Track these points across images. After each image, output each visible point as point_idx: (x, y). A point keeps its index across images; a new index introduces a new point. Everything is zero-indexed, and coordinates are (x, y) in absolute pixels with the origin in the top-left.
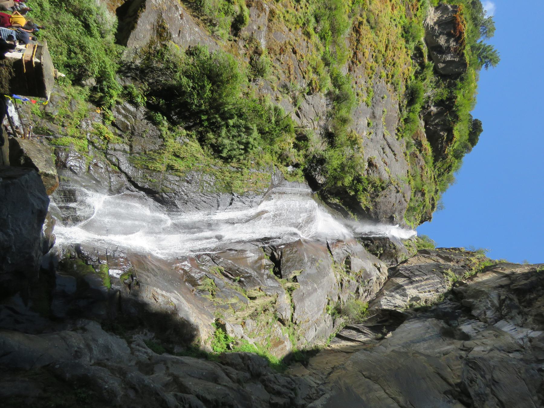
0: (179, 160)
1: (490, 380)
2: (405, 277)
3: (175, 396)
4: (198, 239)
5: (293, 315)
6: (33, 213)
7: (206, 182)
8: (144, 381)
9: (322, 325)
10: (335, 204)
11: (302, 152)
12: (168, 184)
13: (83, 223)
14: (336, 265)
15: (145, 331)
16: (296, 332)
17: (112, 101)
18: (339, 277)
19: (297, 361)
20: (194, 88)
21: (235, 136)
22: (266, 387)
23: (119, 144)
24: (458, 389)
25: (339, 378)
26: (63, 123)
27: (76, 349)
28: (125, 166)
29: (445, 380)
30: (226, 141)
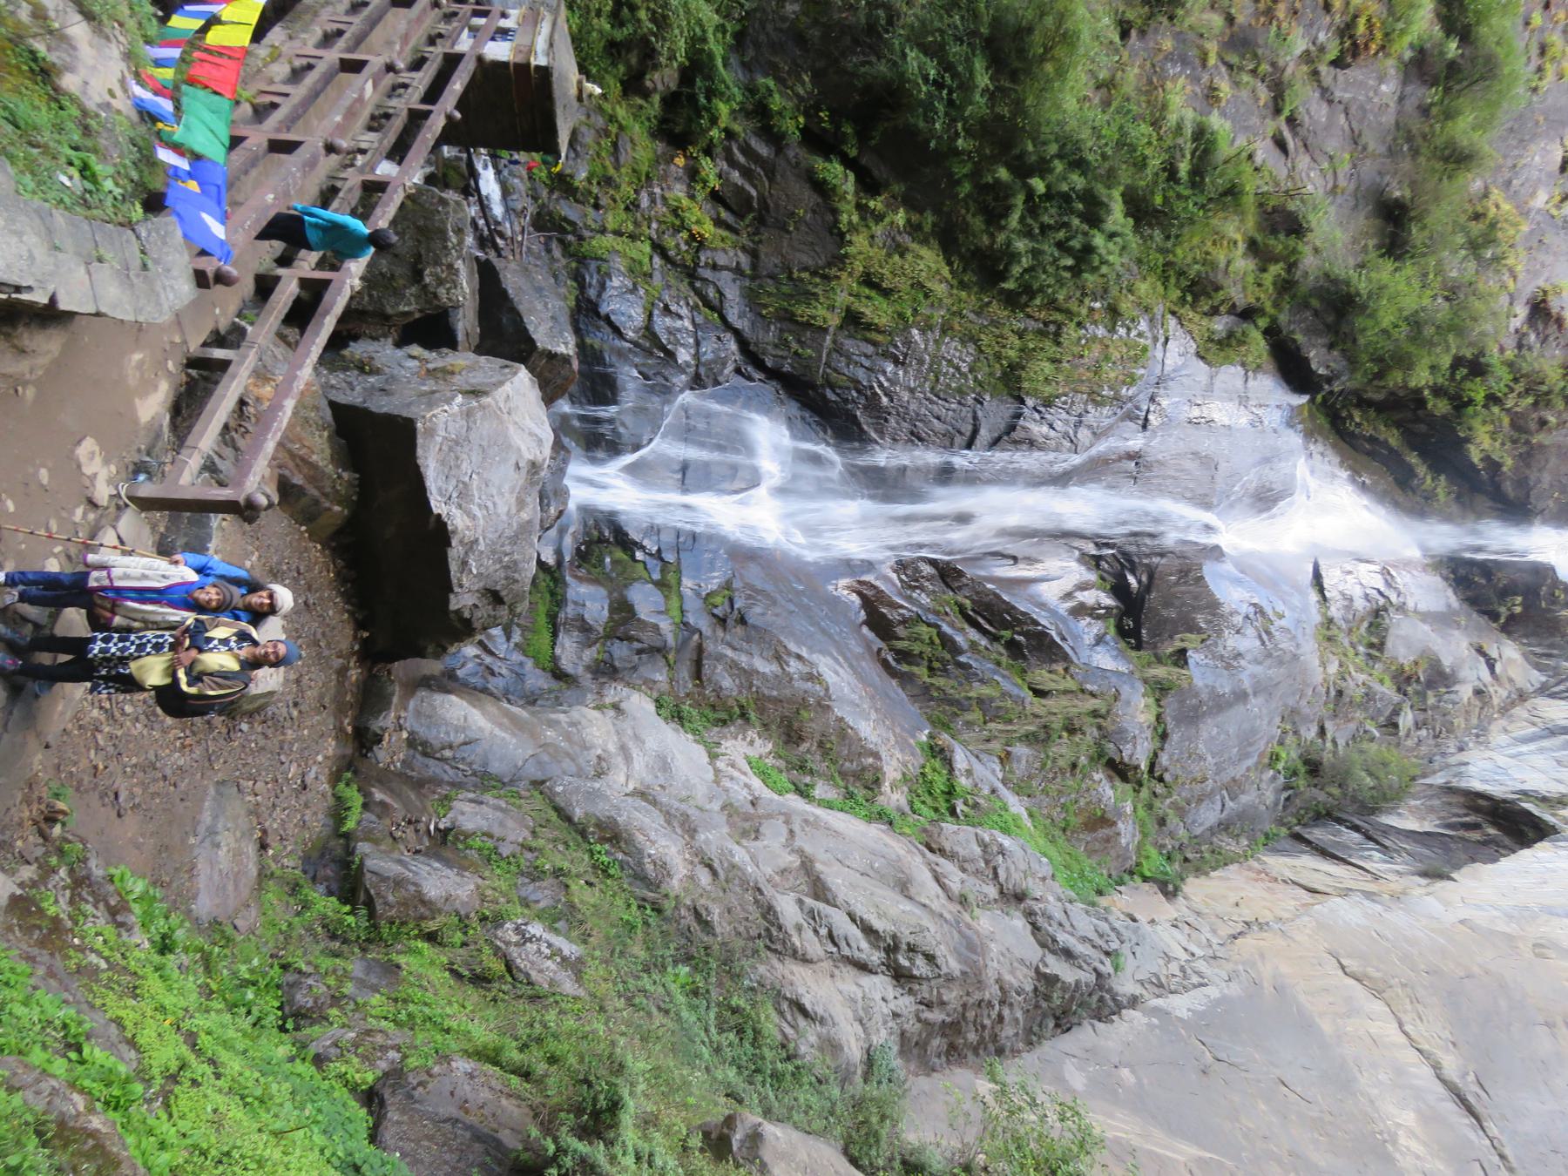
0: (879, 301)
3: (800, 902)
4: (908, 519)
5: (1156, 755)
6: (518, 467)
7: (949, 361)
8: (733, 856)
9: (1244, 799)
10: (1372, 440)
11: (1276, 269)
12: (842, 365)
13: (628, 459)
15: (751, 734)
16: (1157, 803)
17: (714, 133)
18: (1333, 668)
19: (1145, 879)
20: (939, 85)
21: (1050, 227)
22: (1036, 928)
23: (725, 251)
25: (1262, 956)
26: (597, 198)
27: (599, 752)
28: (735, 313)
30: (1021, 245)
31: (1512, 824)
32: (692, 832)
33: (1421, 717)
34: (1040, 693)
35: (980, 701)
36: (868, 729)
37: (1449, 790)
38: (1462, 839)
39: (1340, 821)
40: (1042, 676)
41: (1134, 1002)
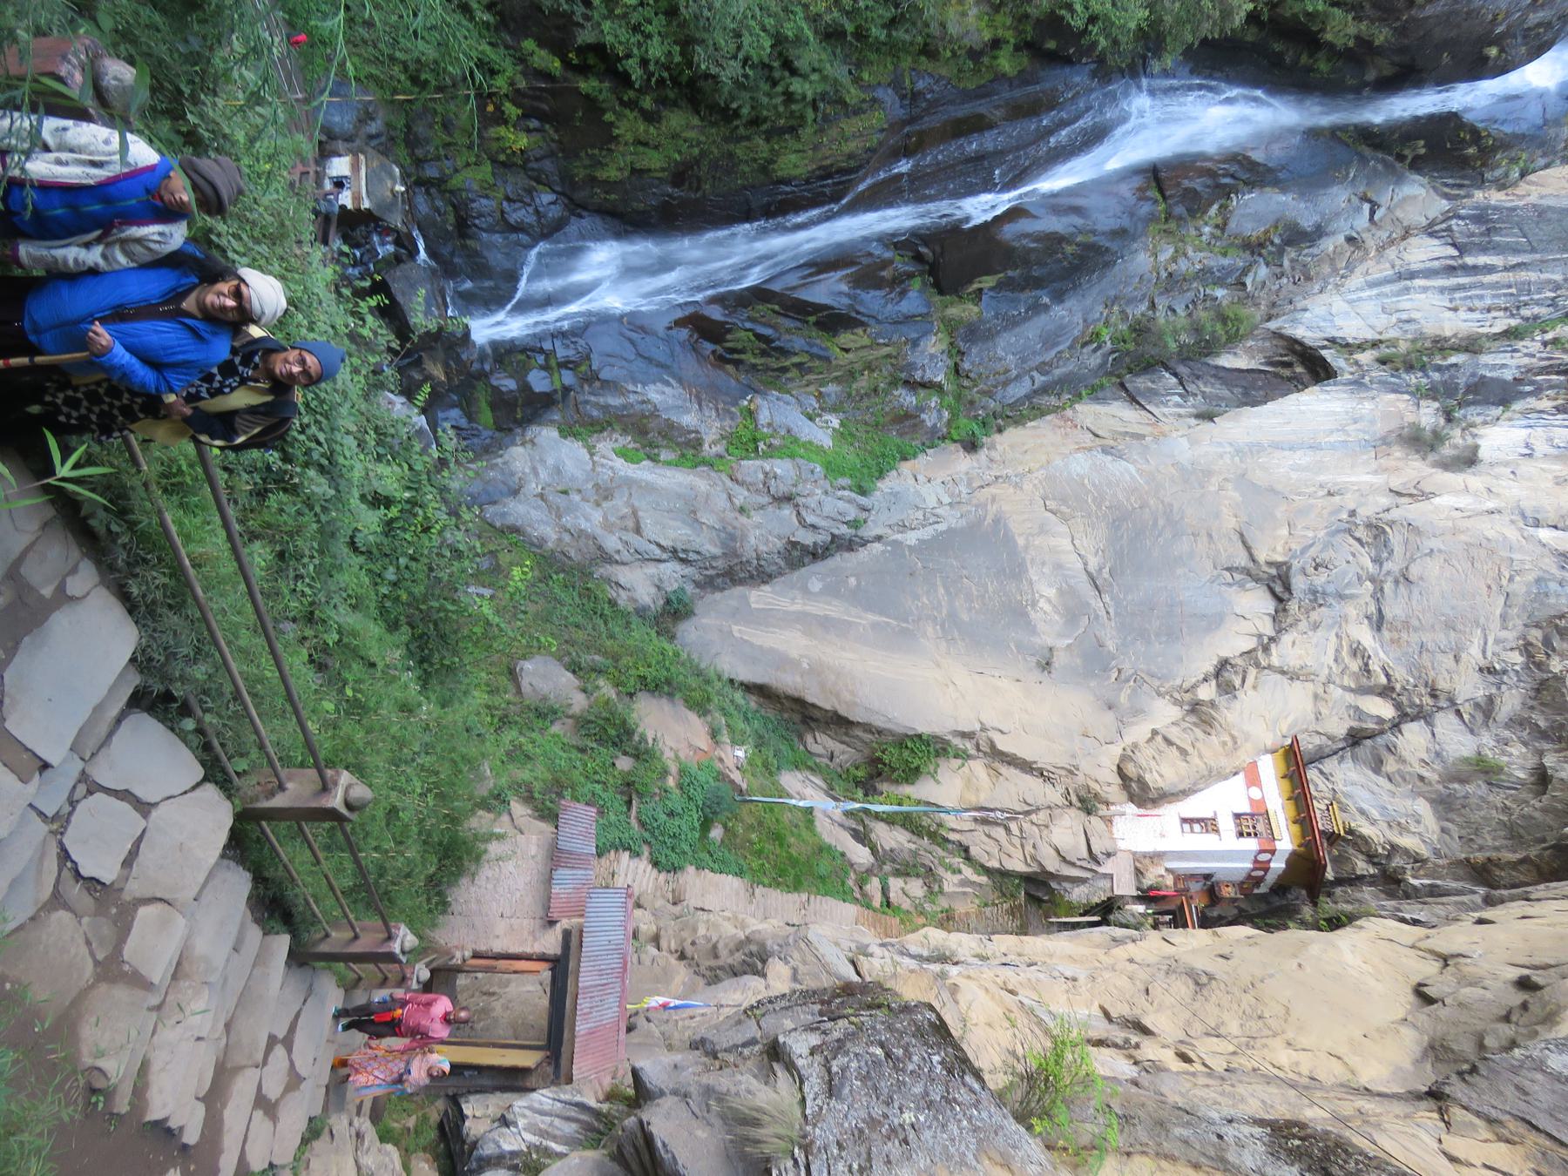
1: (1388, 573)
2: (1454, 245)
14: (1172, 225)
18: (1169, 252)
22: (799, 513)
24: (1273, 571)
25: (994, 499)
29: (1248, 548)
31: (1308, 366)
32: (559, 517)
33: (1278, 270)
34: (847, 351)
35: (799, 366)
36: (689, 420)
37: (1278, 335)
38: (1276, 375)
39: (1167, 369)
40: (845, 338)
41: (879, 538)
